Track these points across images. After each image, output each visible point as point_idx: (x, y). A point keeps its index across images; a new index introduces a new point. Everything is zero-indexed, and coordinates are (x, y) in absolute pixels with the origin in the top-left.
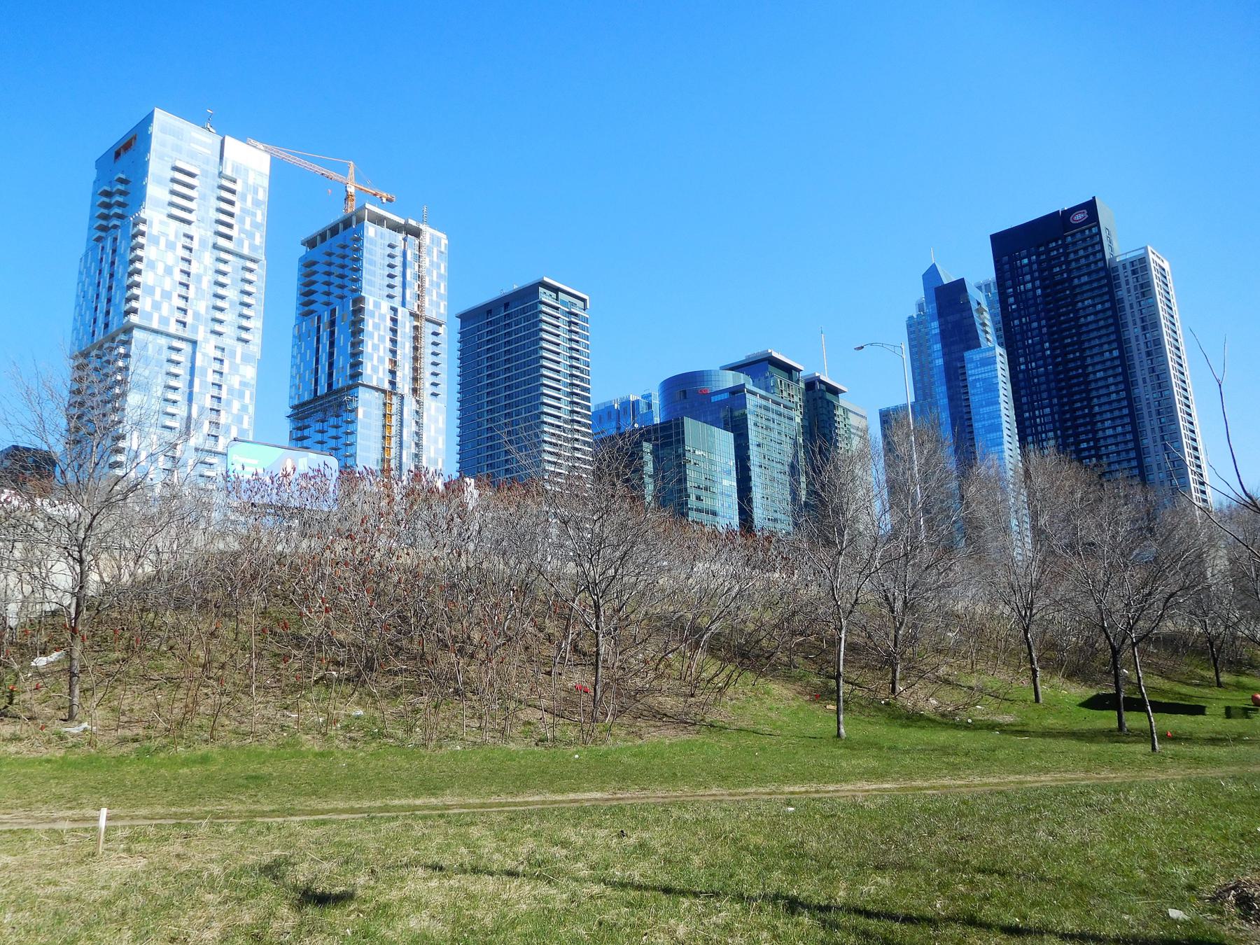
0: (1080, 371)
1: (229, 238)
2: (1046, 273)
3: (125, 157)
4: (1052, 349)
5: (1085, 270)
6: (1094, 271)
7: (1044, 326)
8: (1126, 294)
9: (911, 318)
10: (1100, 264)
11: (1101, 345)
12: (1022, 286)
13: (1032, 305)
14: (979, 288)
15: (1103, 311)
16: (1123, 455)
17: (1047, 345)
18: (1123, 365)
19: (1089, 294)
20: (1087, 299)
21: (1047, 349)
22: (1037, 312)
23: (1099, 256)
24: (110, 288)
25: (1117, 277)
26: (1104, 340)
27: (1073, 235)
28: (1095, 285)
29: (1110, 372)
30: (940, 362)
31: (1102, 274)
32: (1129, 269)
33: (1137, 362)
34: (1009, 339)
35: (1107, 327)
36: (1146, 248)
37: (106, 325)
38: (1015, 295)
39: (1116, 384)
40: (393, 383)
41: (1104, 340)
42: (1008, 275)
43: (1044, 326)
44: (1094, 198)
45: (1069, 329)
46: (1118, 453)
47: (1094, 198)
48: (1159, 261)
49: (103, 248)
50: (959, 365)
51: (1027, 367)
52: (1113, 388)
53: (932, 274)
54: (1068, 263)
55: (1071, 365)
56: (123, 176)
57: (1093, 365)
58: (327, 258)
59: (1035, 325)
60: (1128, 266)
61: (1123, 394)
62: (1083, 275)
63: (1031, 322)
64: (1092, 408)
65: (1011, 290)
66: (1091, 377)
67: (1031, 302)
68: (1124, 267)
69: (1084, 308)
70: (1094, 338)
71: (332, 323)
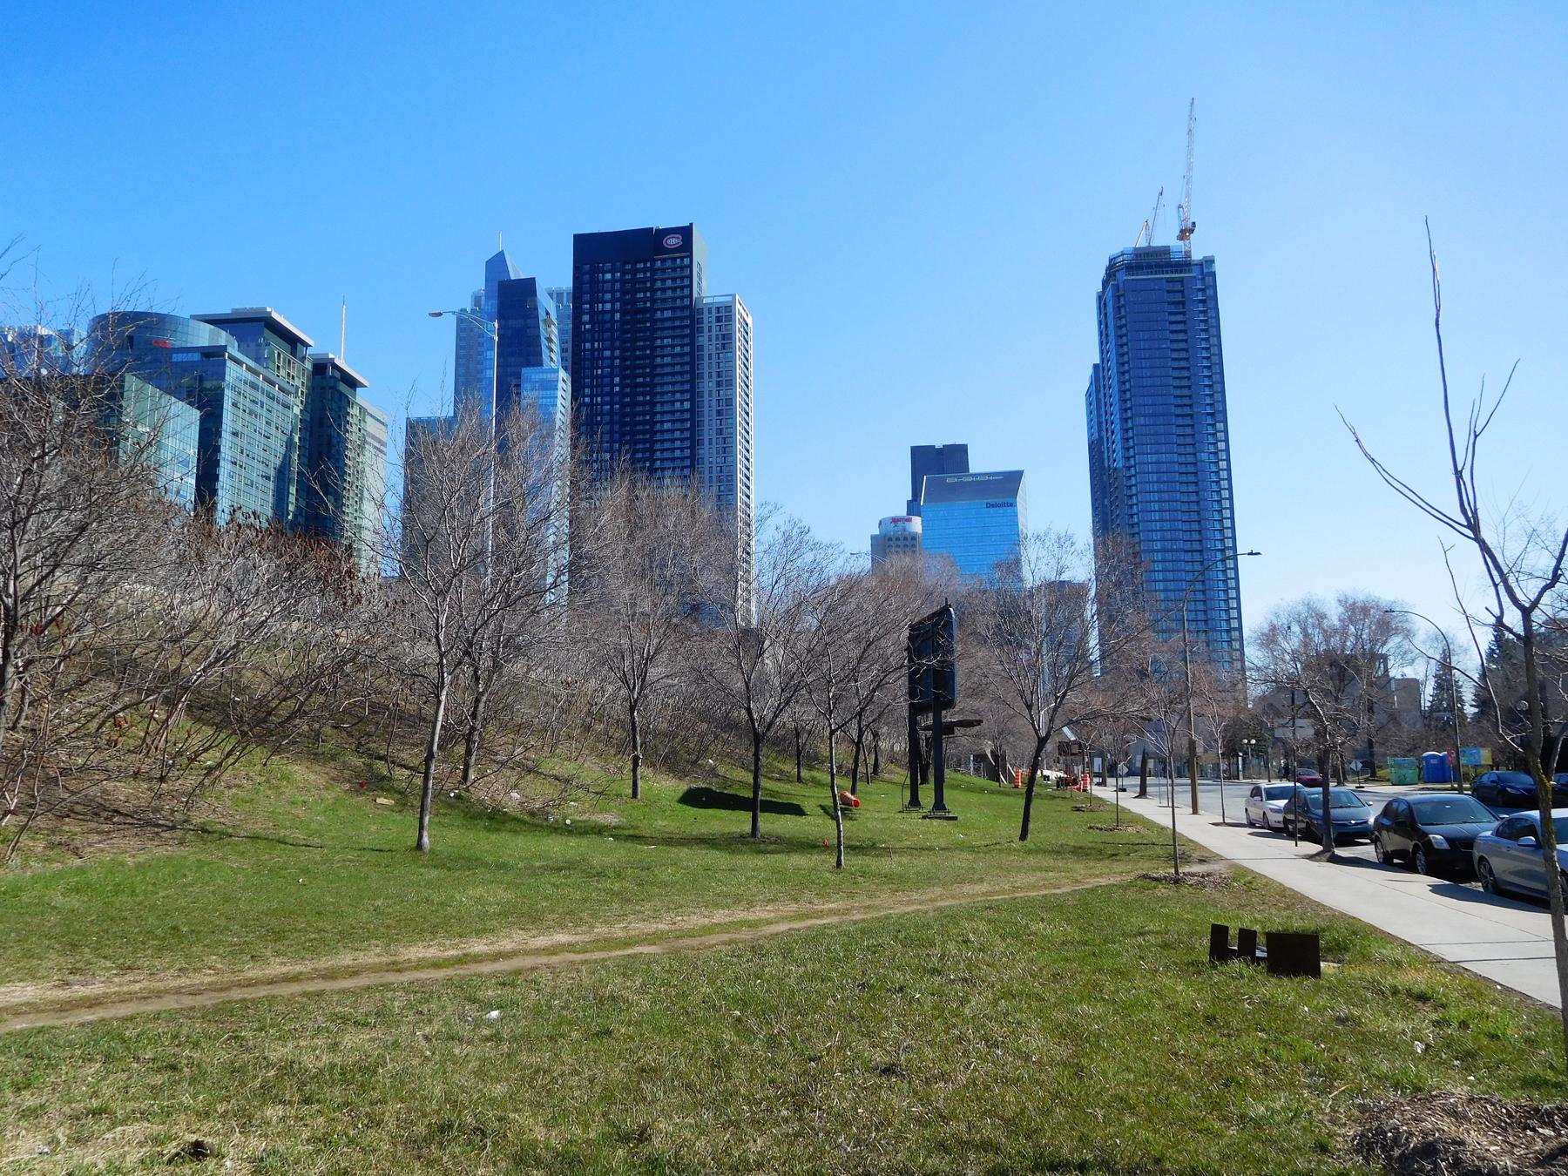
2: (628, 297)
4: (622, 386)
6: (678, 308)
7: (617, 358)
8: (707, 342)
10: (687, 302)
11: (673, 393)
12: (600, 305)
14: (551, 295)
15: (682, 355)
17: (617, 380)
20: (667, 338)
21: (616, 385)
22: (612, 340)
25: (701, 321)
26: (677, 388)
27: (663, 261)
28: (677, 323)
29: (678, 425)
31: (687, 313)
33: (706, 419)
35: (682, 373)
36: (734, 296)
38: (592, 312)
41: (677, 388)
43: (617, 358)
44: (691, 224)
45: (644, 367)
47: (691, 224)
51: (592, 400)
52: (678, 444)
53: (497, 264)
54: (654, 291)
55: (639, 409)
57: (662, 413)
59: (607, 353)
60: (714, 311)
61: (687, 452)
62: (667, 309)
63: (603, 349)
64: (653, 461)
65: (587, 306)
66: (658, 427)
67: (608, 326)
68: (710, 313)
69: (662, 347)
70: (666, 383)
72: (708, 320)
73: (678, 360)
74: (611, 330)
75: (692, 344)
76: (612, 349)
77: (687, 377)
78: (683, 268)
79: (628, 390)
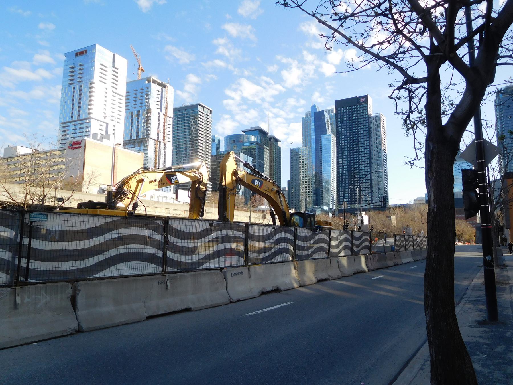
0: (357, 148)
1: (116, 89)
3: (80, 58)
4: (350, 140)
5: (362, 117)
8: (373, 127)
9: (303, 118)
10: (367, 116)
11: (364, 141)
15: (366, 131)
18: (369, 148)
19: (362, 125)
24: (80, 103)
26: (365, 139)
27: (360, 105)
28: (364, 122)
29: (366, 150)
31: (367, 119)
32: (375, 119)
34: (338, 134)
36: (380, 113)
37: (79, 116)
38: (341, 121)
40: (158, 138)
41: (365, 139)
42: (339, 115)
45: (356, 134)
48: (383, 117)
49: (74, 88)
56: (82, 64)
57: (361, 147)
58: (135, 92)
59: (346, 132)
62: (361, 118)
63: (344, 131)
66: (360, 151)
67: (346, 124)
69: (360, 129)
71: (138, 115)
72: (373, 120)
73: (365, 132)
76: (347, 131)
77: (368, 137)
78: (365, 107)
79: (351, 141)
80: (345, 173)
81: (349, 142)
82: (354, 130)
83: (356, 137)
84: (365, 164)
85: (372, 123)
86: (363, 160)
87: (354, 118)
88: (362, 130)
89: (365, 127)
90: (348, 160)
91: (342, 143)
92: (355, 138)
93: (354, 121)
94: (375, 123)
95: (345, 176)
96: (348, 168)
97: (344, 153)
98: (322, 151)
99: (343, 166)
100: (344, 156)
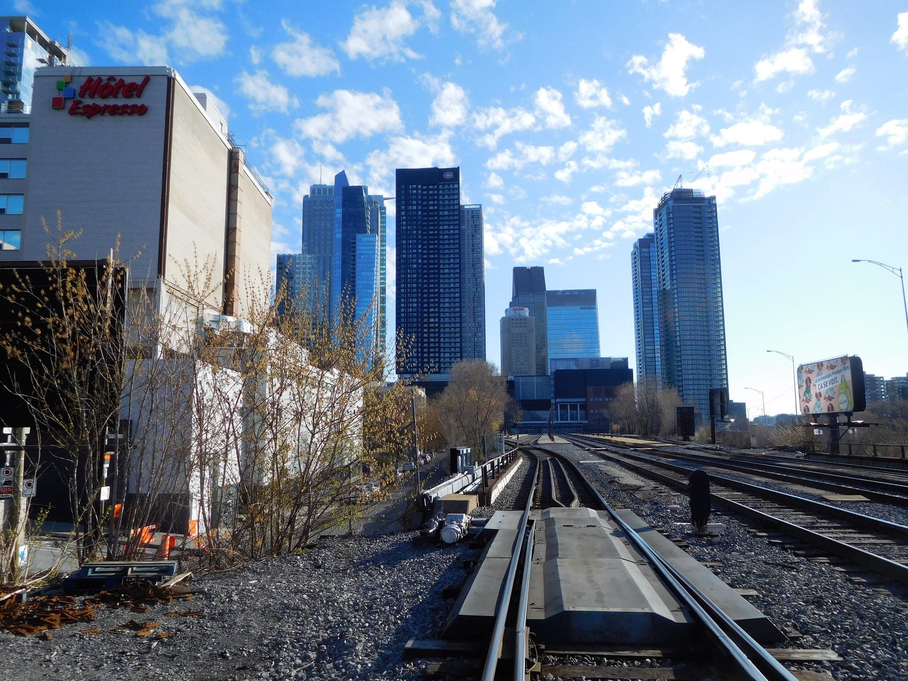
4: (423, 249)
9: (306, 197)
10: (456, 207)
11: (449, 254)
13: (415, 220)
16: (453, 320)
19: (447, 223)
22: (417, 225)
23: (456, 202)
26: (452, 251)
27: (443, 185)
28: (452, 218)
29: (452, 271)
30: (339, 236)
31: (456, 213)
32: (470, 214)
38: (406, 210)
39: (455, 278)
41: (452, 251)
42: (403, 197)
45: (434, 240)
46: (450, 318)
50: (352, 241)
52: (452, 280)
54: (438, 200)
57: (444, 264)
63: (412, 230)
67: (415, 218)
68: (468, 213)
69: (443, 230)
72: (467, 217)
74: (417, 220)
75: (459, 229)
76: (417, 230)
78: (454, 189)
80: (412, 312)
81: (420, 253)
82: (431, 230)
83: (434, 244)
84: (450, 298)
85: (466, 222)
86: (447, 290)
87: (431, 208)
88: (447, 232)
89: (452, 227)
90: (417, 288)
91: (407, 254)
92: (431, 247)
93: (431, 213)
94: (471, 222)
95: (412, 317)
96: (417, 302)
97: (410, 273)
98: (357, 265)
99: (407, 298)
100: (410, 278)
